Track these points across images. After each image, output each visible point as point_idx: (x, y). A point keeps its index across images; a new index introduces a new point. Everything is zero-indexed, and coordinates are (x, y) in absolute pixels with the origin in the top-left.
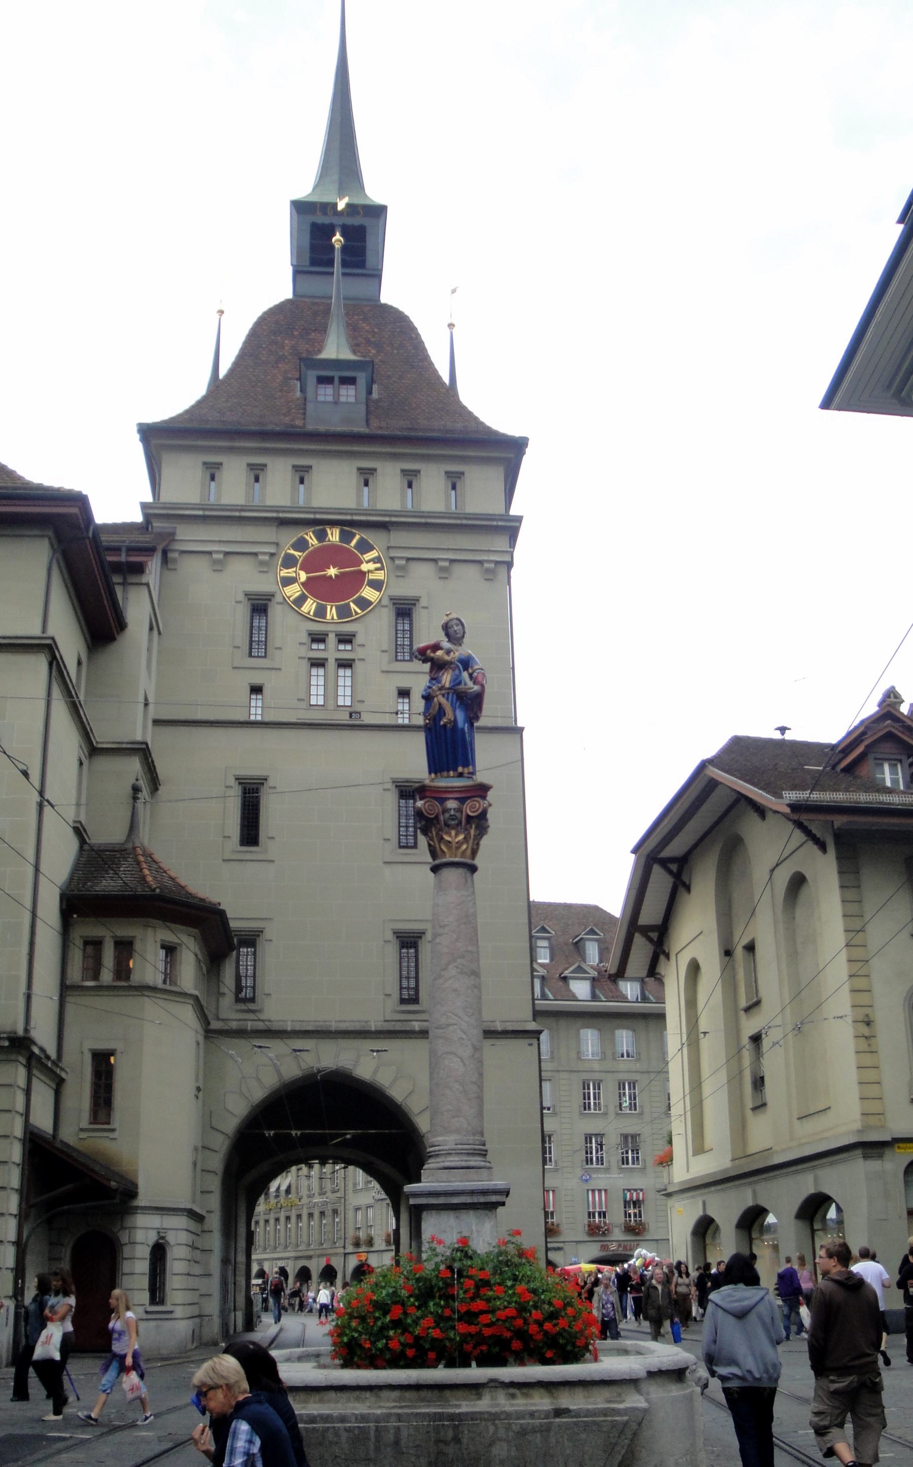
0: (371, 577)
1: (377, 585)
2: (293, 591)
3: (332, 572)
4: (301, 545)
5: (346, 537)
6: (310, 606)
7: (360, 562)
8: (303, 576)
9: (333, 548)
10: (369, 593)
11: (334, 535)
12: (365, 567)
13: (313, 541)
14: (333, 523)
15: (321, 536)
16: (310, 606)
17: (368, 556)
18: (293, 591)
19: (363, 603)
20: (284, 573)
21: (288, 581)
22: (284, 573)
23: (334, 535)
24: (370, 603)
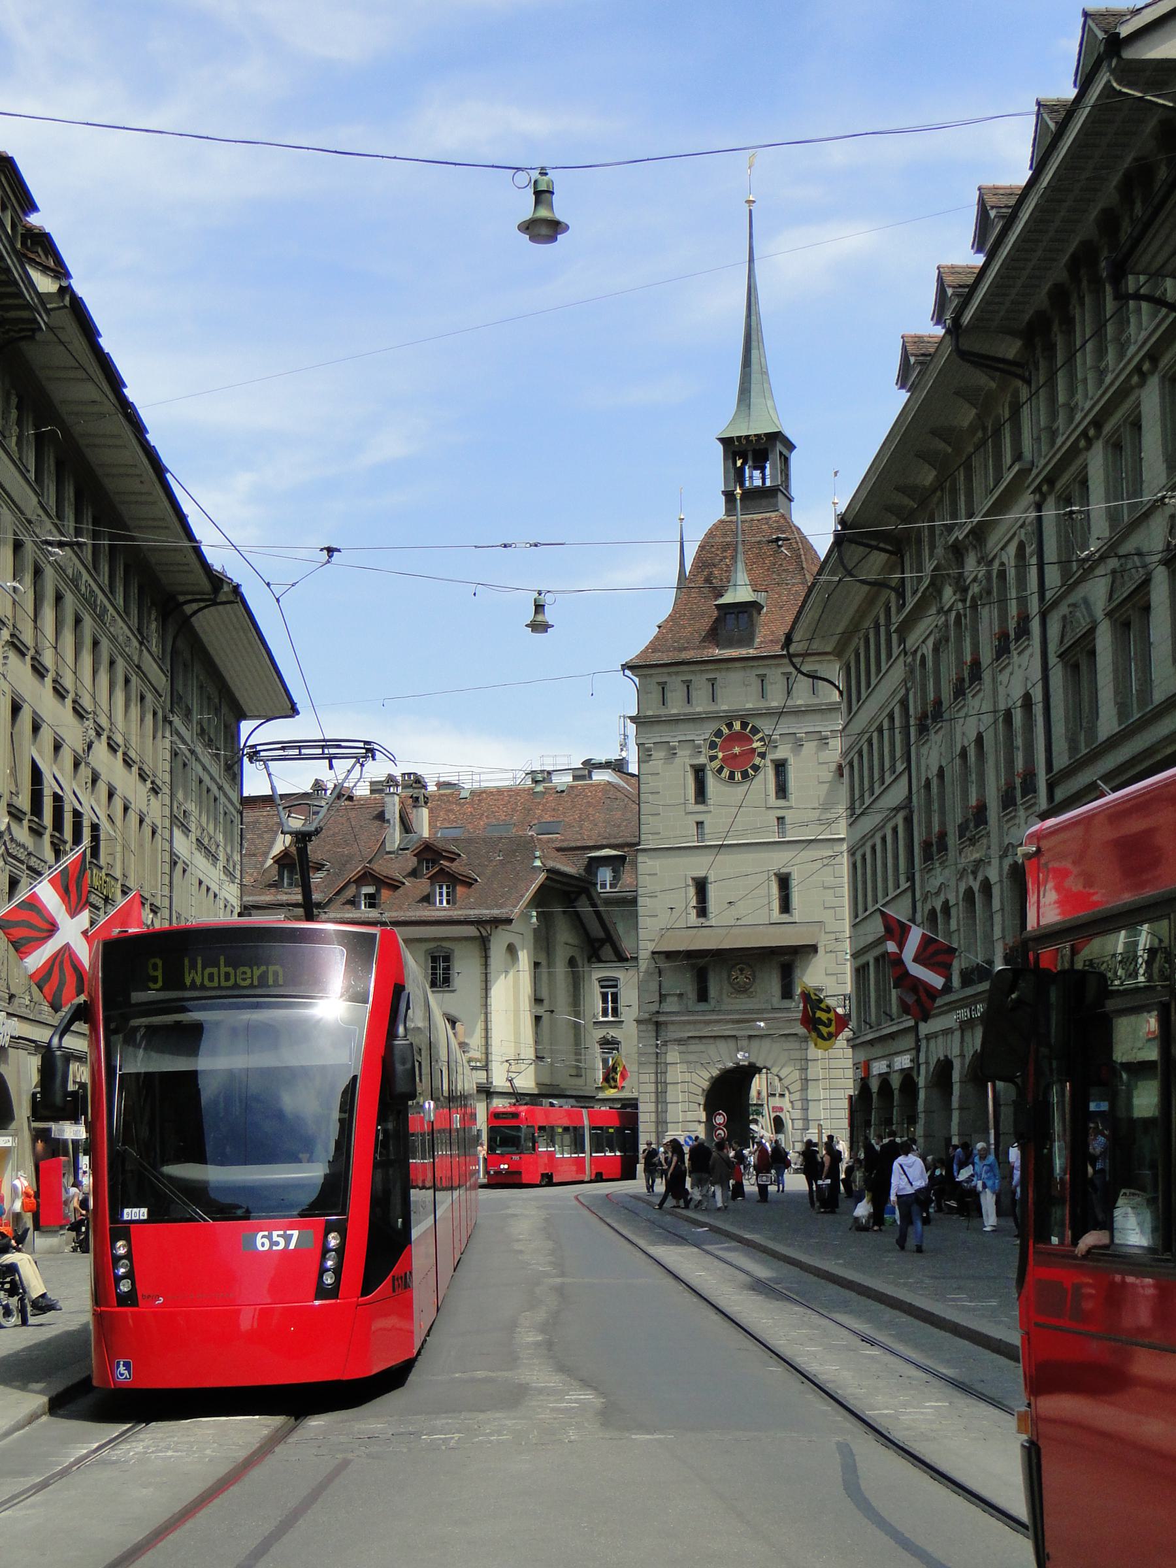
0: (759, 750)
1: (763, 755)
2: (716, 764)
3: (737, 750)
4: (719, 733)
5: (744, 725)
7: (752, 741)
8: (720, 755)
9: (737, 733)
11: (737, 726)
12: (755, 745)
13: (726, 731)
14: (737, 718)
15: (730, 726)
16: (726, 773)
19: (756, 768)
20: (712, 753)
21: (713, 758)
22: (712, 753)
23: (737, 726)
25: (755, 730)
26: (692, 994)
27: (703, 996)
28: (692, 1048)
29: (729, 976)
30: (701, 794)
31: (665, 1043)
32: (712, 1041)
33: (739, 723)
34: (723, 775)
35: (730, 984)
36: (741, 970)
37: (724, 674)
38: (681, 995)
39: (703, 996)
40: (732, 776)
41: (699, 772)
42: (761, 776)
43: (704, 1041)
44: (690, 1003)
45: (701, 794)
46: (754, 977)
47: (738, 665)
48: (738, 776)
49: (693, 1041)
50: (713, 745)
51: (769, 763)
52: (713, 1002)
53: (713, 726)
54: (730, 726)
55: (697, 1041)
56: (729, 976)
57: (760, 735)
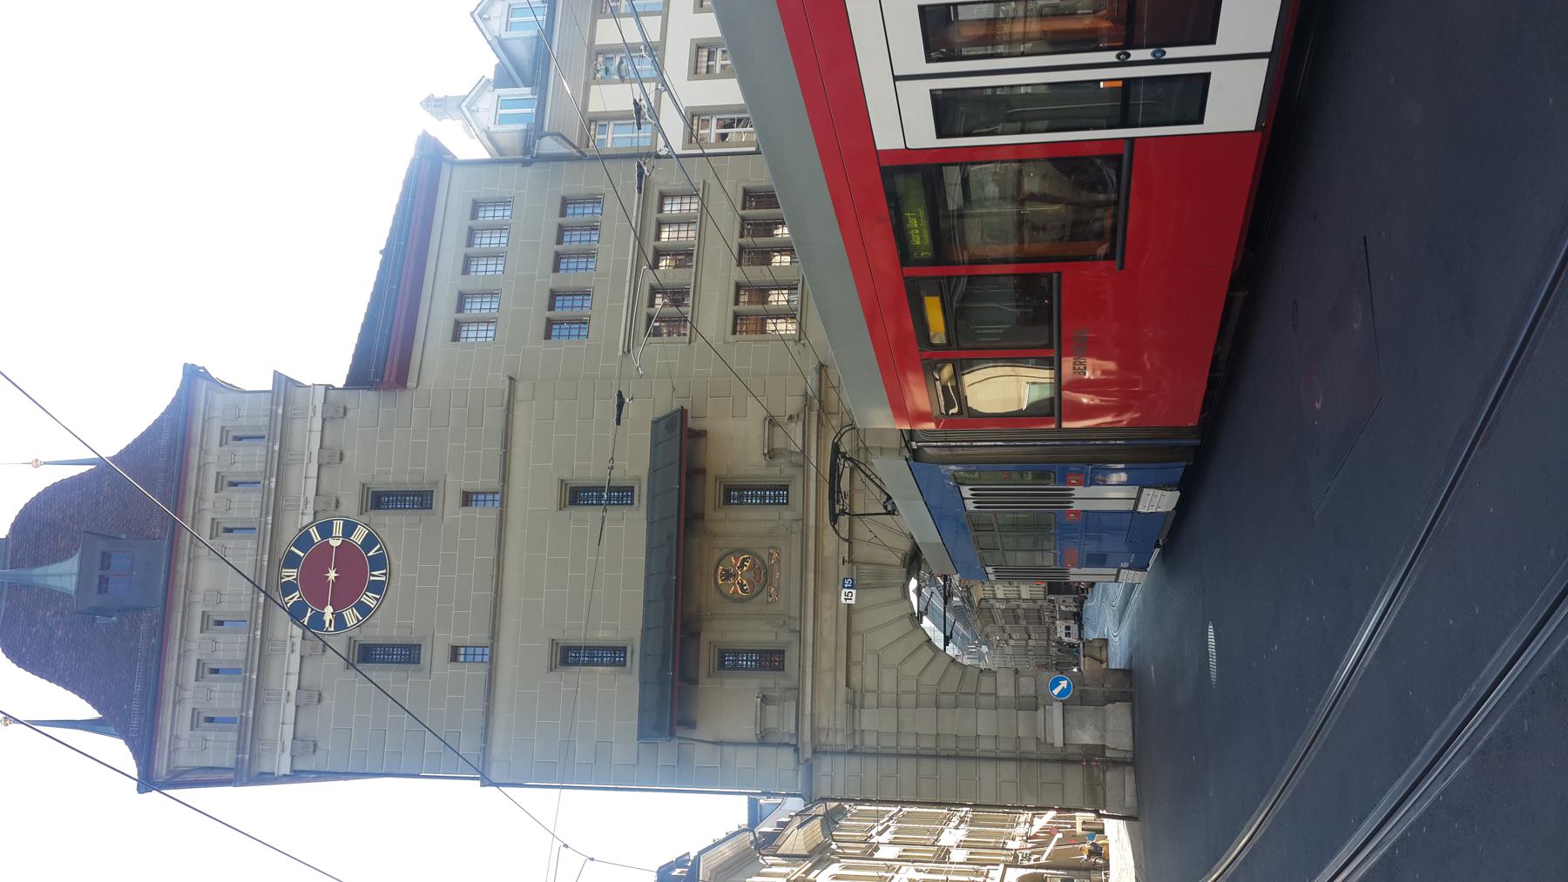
1: (349, 528)
2: (351, 616)
3: (332, 575)
5: (291, 561)
6: (369, 599)
9: (303, 576)
10: (358, 537)
15: (288, 588)
17: (316, 537)
18: (351, 616)
19: (370, 541)
21: (340, 623)
23: (291, 574)
24: (370, 534)
25: (304, 540)
26: (769, 680)
27: (771, 660)
28: (870, 681)
29: (741, 600)
30: (408, 654)
31: (854, 732)
32: (856, 641)
33: (286, 572)
34: (372, 603)
35: (748, 599)
36: (728, 575)
37: (198, 598)
38: (765, 700)
39: (771, 660)
40: (377, 588)
41: (367, 654)
42: (384, 534)
43: (856, 656)
44: (784, 683)
45: (408, 654)
46: (743, 551)
47: (182, 567)
48: (378, 576)
49: (855, 679)
50: (318, 621)
51: (365, 518)
52: (785, 636)
53: (282, 617)
54: (288, 588)
55: (856, 671)
56: (741, 600)
57: (314, 532)
